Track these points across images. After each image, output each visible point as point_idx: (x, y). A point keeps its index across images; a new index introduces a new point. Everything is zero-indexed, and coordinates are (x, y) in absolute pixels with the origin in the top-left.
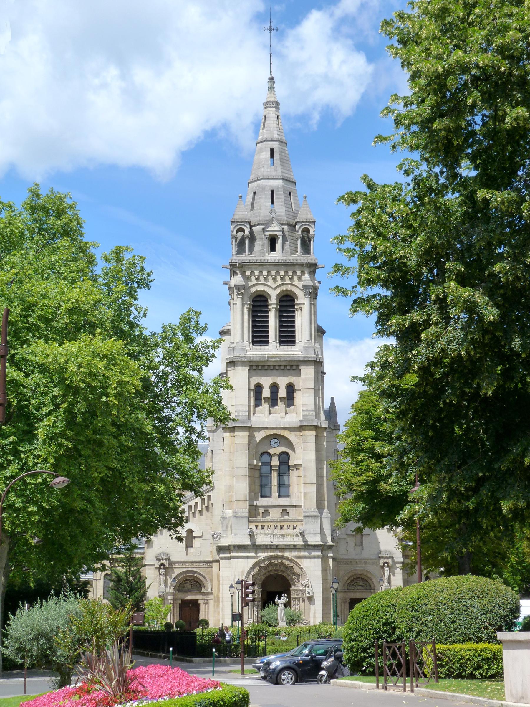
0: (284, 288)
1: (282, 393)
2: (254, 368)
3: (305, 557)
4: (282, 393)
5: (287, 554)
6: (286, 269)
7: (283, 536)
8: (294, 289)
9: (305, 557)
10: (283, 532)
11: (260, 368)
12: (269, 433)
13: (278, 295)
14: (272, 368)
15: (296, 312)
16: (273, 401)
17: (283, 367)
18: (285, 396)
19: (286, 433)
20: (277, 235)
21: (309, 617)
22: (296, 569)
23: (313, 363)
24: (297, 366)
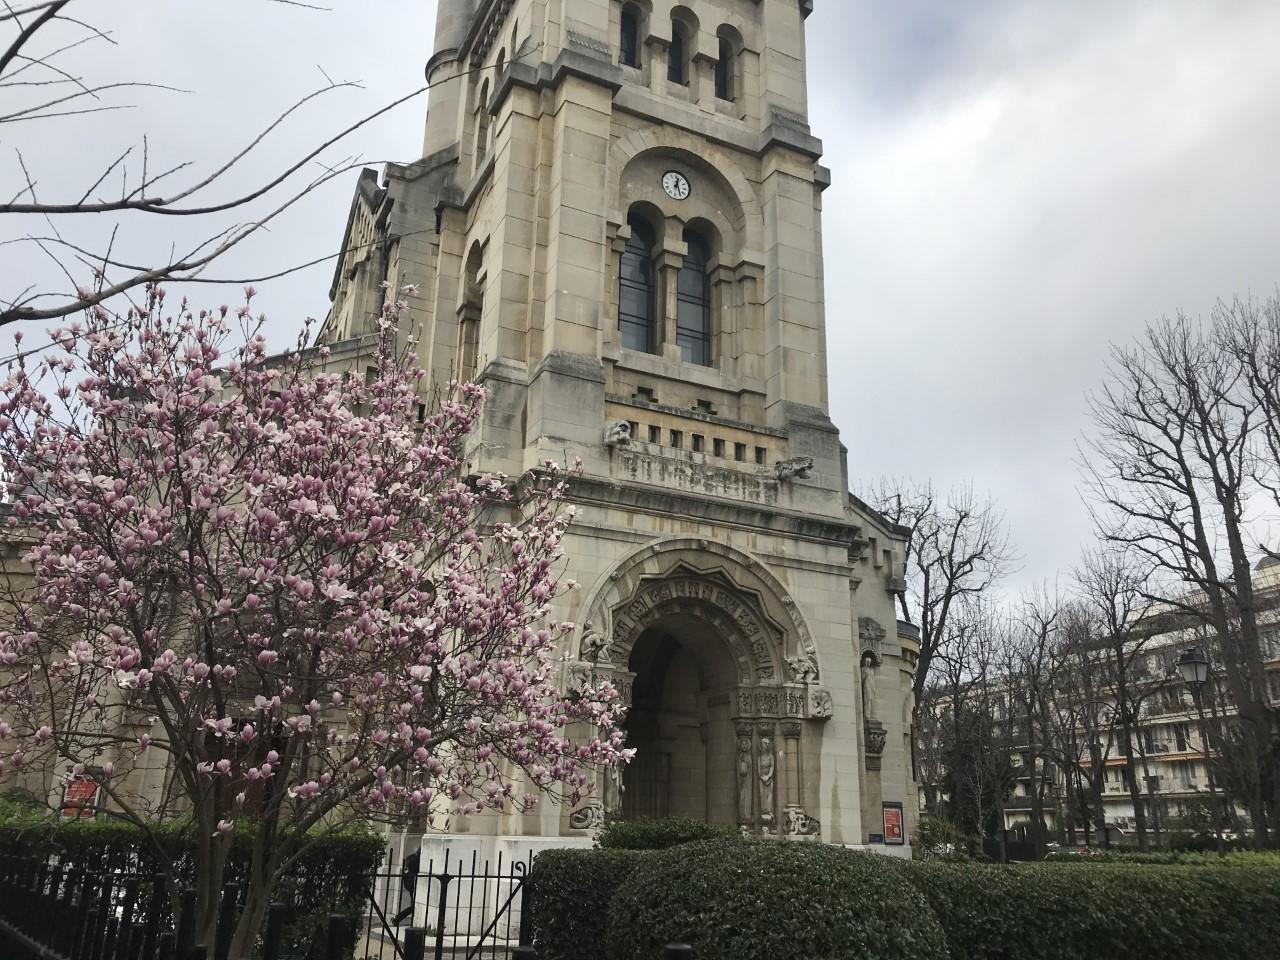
1: (707, 44)
3: (800, 564)
4: (707, 44)
5: (740, 542)
7: (727, 476)
9: (800, 564)
10: (721, 463)
12: (668, 143)
16: (679, 58)
19: (718, 160)
21: (817, 805)
22: (771, 608)
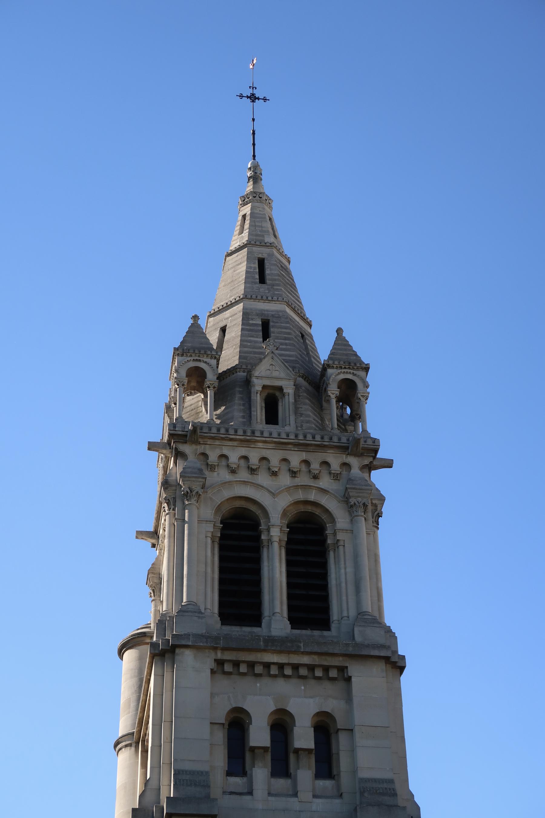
0: (300, 496)
2: (228, 668)
6: (304, 456)
8: (324, 500)
11: (243, 668)
13: (285, 513)
14: (274, 670)
15: (332, 554)
17: (303, 672)
18: (311, 745)
20: (280, 389)
23: (382, 665)
24: (342, 669)
